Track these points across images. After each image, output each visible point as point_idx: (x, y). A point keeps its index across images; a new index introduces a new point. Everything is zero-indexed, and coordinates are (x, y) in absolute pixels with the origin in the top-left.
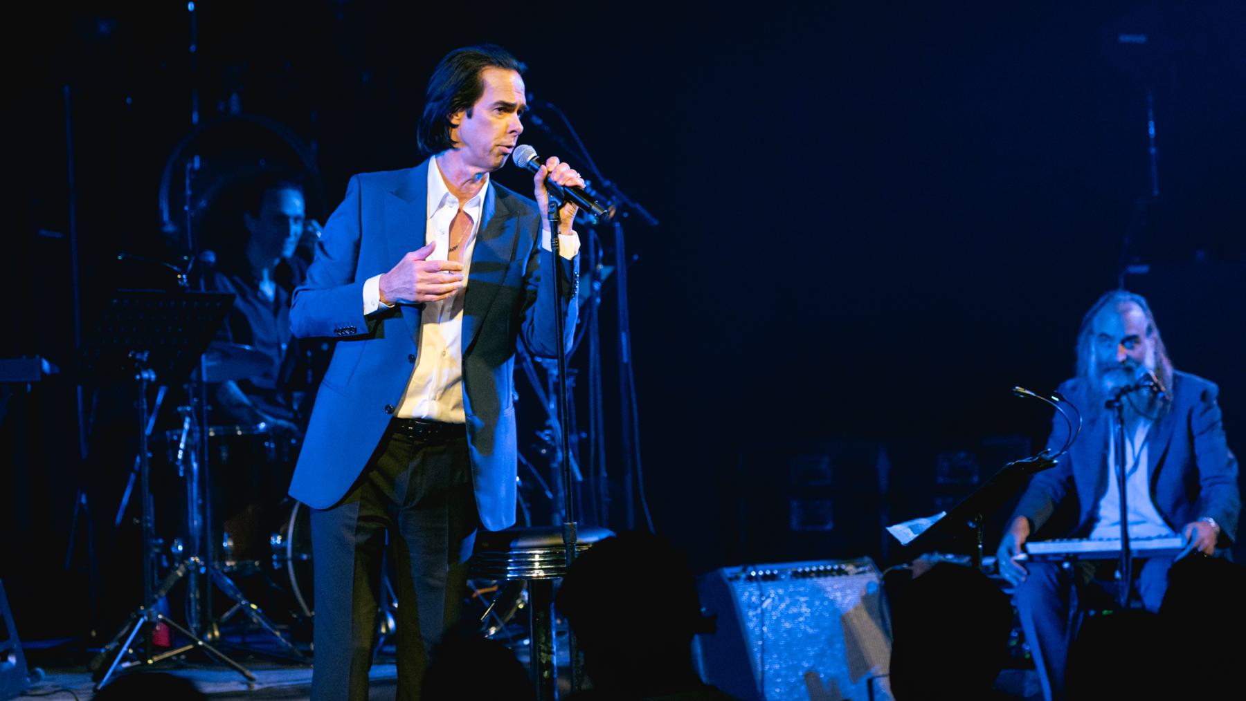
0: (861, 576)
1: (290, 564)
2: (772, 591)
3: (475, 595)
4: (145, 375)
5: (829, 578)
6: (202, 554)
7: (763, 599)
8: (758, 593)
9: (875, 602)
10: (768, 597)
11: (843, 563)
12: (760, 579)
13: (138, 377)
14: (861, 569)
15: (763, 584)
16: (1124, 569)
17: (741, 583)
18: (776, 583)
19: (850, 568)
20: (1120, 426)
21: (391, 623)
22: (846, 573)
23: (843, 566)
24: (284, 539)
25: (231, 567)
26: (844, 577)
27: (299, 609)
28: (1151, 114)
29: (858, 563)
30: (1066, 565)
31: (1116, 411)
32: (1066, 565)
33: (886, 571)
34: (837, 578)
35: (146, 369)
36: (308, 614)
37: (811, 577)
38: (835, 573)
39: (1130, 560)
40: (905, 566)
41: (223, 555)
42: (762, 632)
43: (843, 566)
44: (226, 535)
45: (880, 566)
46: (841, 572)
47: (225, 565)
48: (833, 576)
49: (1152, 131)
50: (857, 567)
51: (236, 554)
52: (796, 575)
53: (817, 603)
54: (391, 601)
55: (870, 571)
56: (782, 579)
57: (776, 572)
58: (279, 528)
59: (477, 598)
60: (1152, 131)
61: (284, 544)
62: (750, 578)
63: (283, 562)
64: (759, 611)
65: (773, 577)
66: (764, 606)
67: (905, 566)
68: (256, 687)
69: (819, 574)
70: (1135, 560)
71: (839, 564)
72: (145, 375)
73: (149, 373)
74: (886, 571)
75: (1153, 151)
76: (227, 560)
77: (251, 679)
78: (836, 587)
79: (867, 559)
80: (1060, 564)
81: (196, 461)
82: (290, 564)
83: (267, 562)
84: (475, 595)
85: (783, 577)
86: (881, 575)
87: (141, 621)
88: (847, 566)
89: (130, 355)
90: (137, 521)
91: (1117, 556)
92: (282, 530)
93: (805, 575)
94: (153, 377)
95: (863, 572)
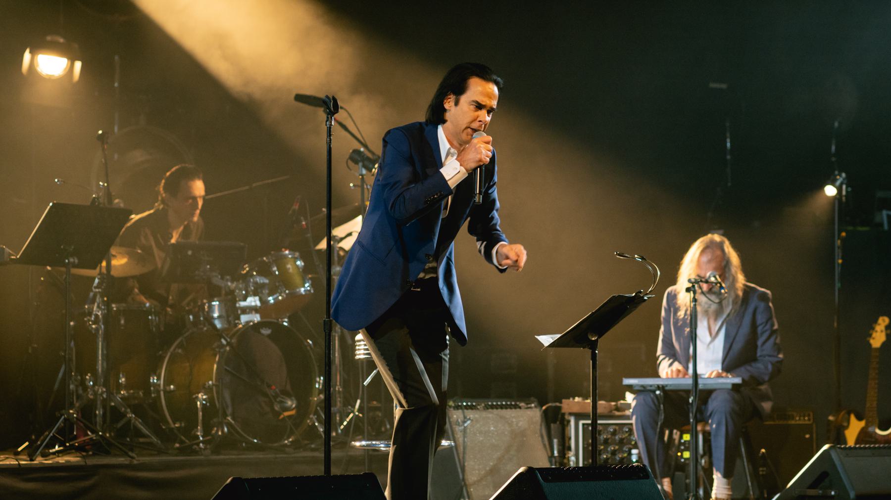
0: (529, 410)
1: (162, 393)
2: (470, 414)
3: (282, 416)
4: (72, 260)
5: (509, 410)
6: (105, 385)
7: (466, 420)
8: (462, 416)
9: (538, 427)
10: (469, 419)
11: (518, 401)
12: (463, 408)
13: (67, 261)
14: (529, 406)
15: (465, 411)
16: (694, 394)
17: (452, 409)
18: (474, 411)
19: (522, 404)
20: (694, 303)
21: (226, 429)
22: (520, 408)
23: (518, 403)
24: (158, 379)
25: (124, 394)
26: (518, 410)
27: (168, 422)
28: (728, 135)
29: (528, 402)
30: (658, 392)
31: (692, 292)
32: (658, 392)
33: (544, 408)
34: (514, 410)
35: (72, 256)
36: (172, 426)
37: (497, 408)
38: (512, 407)
39: (698, 391)
40: (558, 404)
41: (119, 387)
42: (464, 442)
43: (518, 403)
44: (121, 376)
45: (541, 404)
46: (516, 407)
47: (121, 393)
48: (511, 408)
49: (728, 145)
50: (527, 404)
51: (127, 387)
52: (487, 407)
53: (500, 425)
54: (225, 415)
55: (536, 407)
56: (478, 409)
57: (474, 404)
58: (155, 371)
59: (284, 418)
60: (728, 145)
61: (159, 382)
62: (457, 407)
63: (158, 392)
64: (463, 427)
65: (472, 407)
66: (466, 425)
67: (558, 404)
68: (135, 462)
69: (502, 407)
70: (702, 391)
71: (515, 401)
72: (72, 260)
73: (74, 259)
74: (544, 408)
75: (729, 157)
76: (122, 390)
77: (132, 458)
78: (513, 415)
79: (532, 398)
80: (654, 392)
81: (103, 324)
82: (162, 393)
83: (148, 392)
84: (282, 416)
85: (479, 407)
86: (542, 410)
87: (63, 417)
88: (520, 403)
89: (62, 247)
90: (63, 354)
91: (690, 388)
92: (158, 372)
93: (492, 407)
94: (76, 261)
95: (531, 408)
